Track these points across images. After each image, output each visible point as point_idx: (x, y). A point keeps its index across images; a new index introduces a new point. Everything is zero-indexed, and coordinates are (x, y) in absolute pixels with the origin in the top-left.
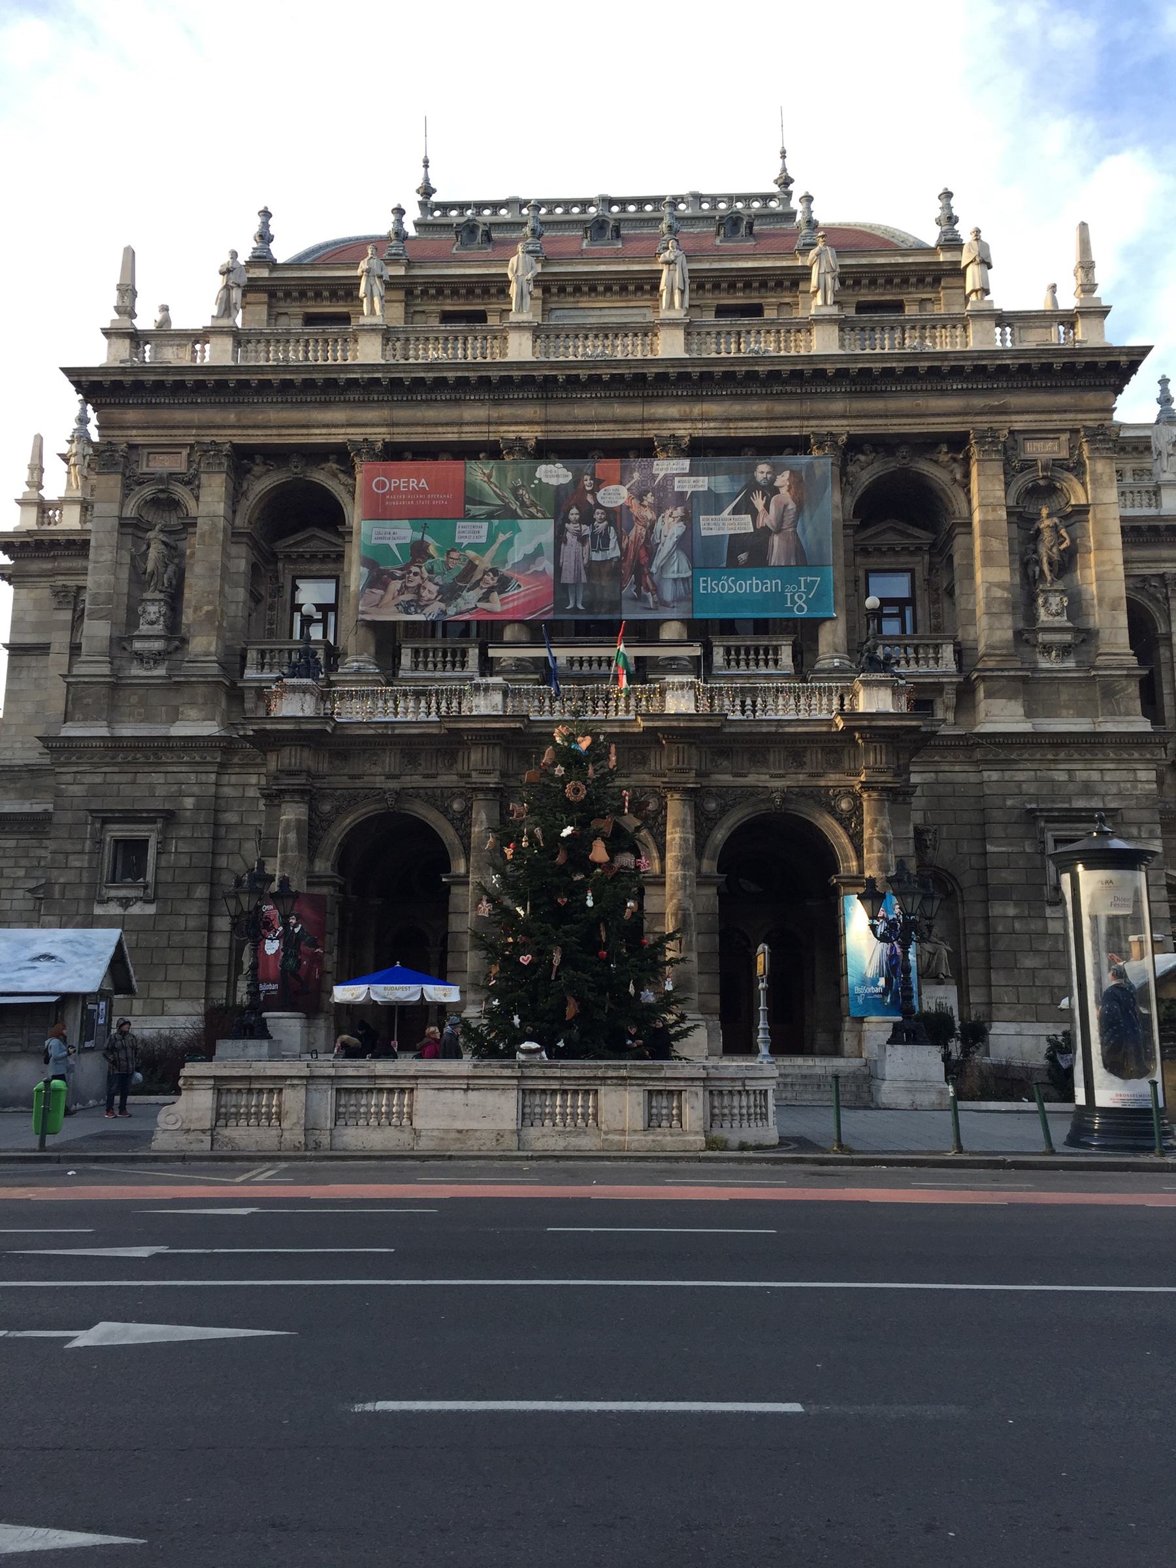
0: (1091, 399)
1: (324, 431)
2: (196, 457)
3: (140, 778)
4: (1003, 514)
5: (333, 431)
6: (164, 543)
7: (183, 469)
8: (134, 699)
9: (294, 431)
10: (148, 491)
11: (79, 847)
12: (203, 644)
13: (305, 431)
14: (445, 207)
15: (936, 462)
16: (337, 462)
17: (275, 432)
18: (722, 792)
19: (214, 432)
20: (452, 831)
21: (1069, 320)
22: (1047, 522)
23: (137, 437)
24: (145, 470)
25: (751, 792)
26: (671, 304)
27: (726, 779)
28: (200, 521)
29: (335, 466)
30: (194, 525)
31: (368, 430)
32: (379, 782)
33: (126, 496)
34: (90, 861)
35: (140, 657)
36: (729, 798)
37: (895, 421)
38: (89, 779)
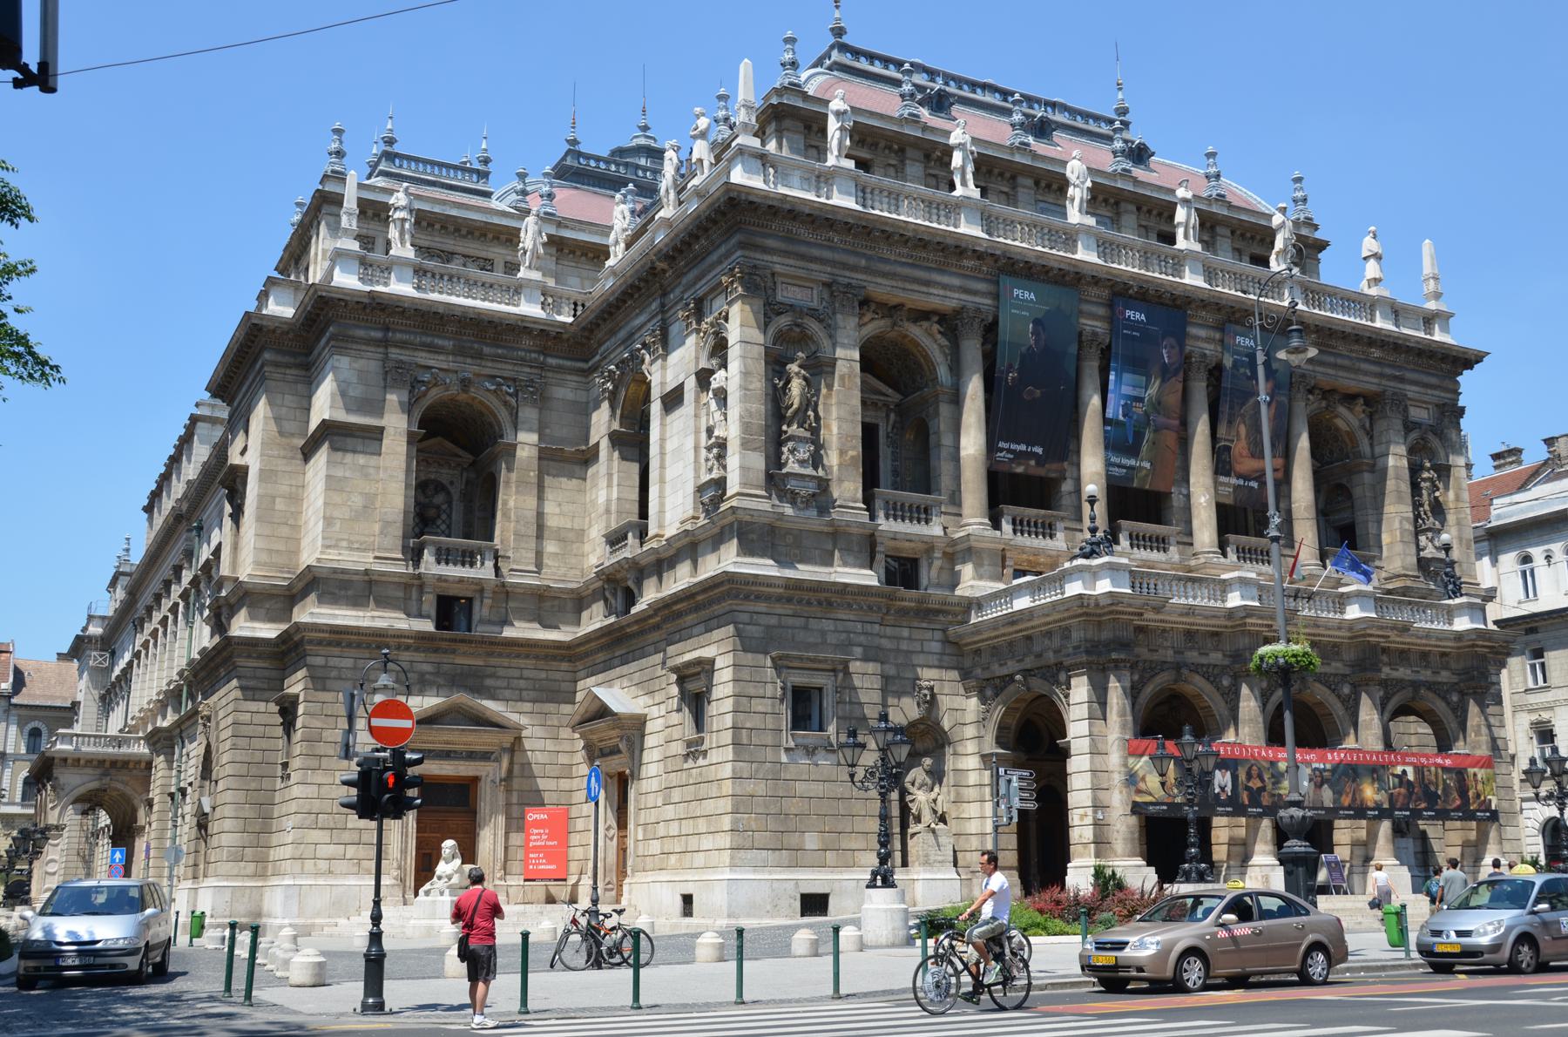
0: (1447, 383)
1: (941, 292)
2: (826, 296)
3: (813, 623)
4: (1405, 462)
5: (949, 294)
6: (805, 379)
7: (815, 304)
8: (790, 539)
9: (916, 287)
10: (784, 321)
11: (761, 692)
12: (848, 490)
13: (924, 289)
14: (857, 53)
15: (1351, 410)
16: (938, 322)
17: (900, 284)
18: (1384, 684)
19: (847, 273)
20: (1223, 704)
21: (1429, 320)
22: (1426, 475)
23: (778, 264)
24: (779, 298)
25: (1400, 684)
26: (1186, 237)
27: (1386, 671)
28: (839, 363)
29: (936, 327)
30: (834, 365)
31: (977, 299)
32: (1169, 655)
33: (766, 325)
34: (773, 706)
35: (792, 498)
36: (1390, 687)
37: (1341, 373)
38: (764, 620)
